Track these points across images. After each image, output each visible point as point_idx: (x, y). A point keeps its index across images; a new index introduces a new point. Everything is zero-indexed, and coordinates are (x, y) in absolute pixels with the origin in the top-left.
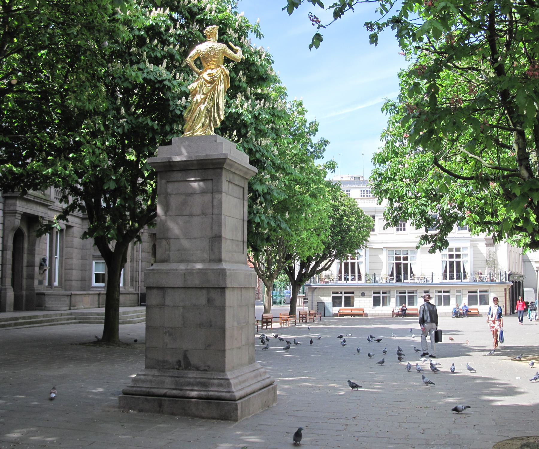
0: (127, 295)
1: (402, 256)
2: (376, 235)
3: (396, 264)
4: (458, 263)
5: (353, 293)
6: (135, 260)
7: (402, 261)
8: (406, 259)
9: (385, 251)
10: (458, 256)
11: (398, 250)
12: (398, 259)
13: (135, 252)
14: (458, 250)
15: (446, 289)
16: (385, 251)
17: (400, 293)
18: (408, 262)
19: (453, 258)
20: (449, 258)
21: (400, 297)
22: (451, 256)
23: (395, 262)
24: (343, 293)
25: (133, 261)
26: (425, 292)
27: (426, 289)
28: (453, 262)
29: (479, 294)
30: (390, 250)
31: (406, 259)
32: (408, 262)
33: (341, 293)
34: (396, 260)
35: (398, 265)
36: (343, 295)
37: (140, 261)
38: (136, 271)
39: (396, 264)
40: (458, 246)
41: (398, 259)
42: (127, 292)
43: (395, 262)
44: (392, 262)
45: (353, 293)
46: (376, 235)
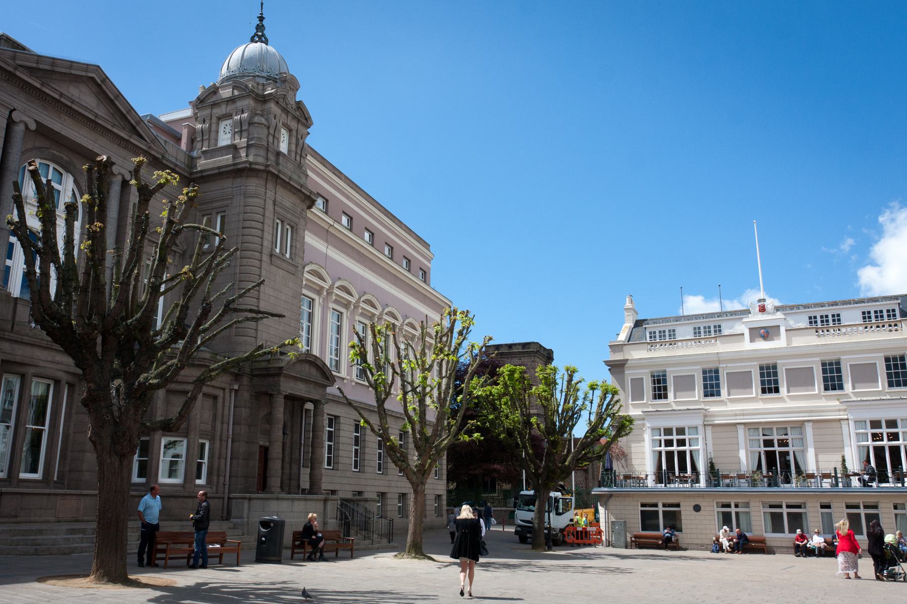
0: (186, 500)
1: (775, 437)
6: (218, 438)
7: (777, 448)
9: (741, 430)
10: (895, 436)
11: (767, 428)
12: (769, 443)
13: (218, 424)
16: (741, 430)
17: (771, 506)
18: (790, 449)
21: (772, 514)
22: (876, 437)
23: (763, 449)
24: (660, 505)
25: (214, 440)
26: (822, 507)
28: (883, 448)
30: (751, 427)
32: (790, 449)
35: (770, 456)
37: (230, 440)
38: (219, 458)
40: (891, 416)
41: (769, 443)
42: (186, 494)
43: (763, 449)
44: (759, 449)
45: (678, 505)
46: (722, 401)
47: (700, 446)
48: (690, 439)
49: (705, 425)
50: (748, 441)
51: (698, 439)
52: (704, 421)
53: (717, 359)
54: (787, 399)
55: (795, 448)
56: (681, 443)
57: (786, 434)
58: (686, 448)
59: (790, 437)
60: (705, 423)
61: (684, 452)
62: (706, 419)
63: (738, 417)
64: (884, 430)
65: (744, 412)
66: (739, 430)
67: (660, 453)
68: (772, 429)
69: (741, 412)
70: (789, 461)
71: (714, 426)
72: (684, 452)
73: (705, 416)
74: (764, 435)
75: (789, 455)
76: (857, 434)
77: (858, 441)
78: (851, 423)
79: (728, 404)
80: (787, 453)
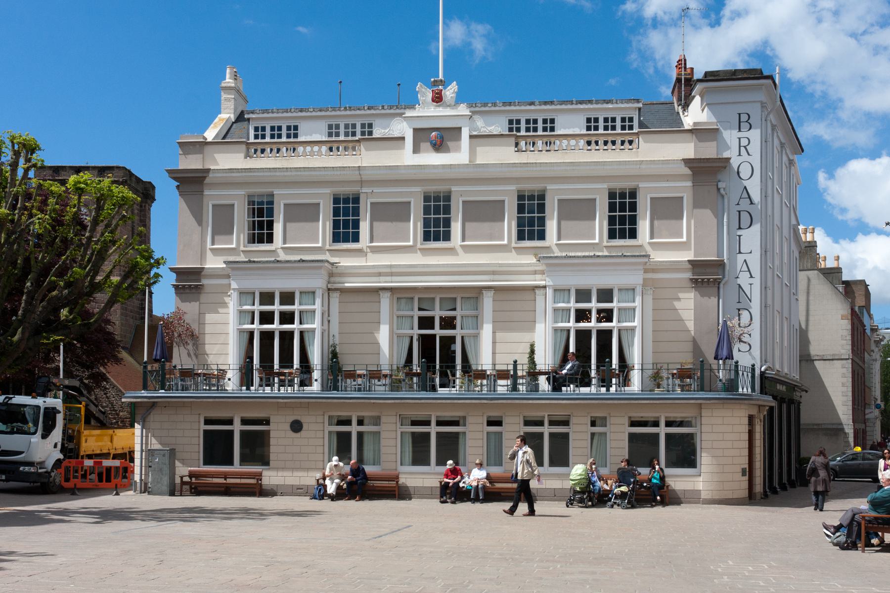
1: (438, 313)
2: (360, 251)
3: (423, 338)
4: (605, 337)
5: (267, 422)
7: (438, 331)
8: (448, 323)
9: (385, 301)
10: (606, 314)
12: (426, 322)
14: (606, 295)
15: (559, 413)
16: (385, 301)
18: (457, 333)
19: (588, 319)
20: (578, 320)
22: (582, 315)
23: (416, 332)
27: (495, 414)
29: (662, 431)
31: (448, 323)
32: (457, 333)
33: (230, 422)
34: (421, 327)
35: (427, 342)
36: (237, 428)
39: (423, 338)
43: (416, 332)
44: (410, 332)
46: (360, 251)
47: (315, 325)
48: (301, 312)
49: (329, 290)
50: (395, 318)
51: (314, 312)
52: (329, 283)
53: (358, 178)
54: (460, 250)
55: (464, 332)
56: (287, 318)
57: (455, 309)
58: (295, 327)
59: (458, 313)
60: (330, 286)
61: (291, 334)
62: (332, 279)
63: (382, 278)
64: (594, 305)
65: (394, 270)
66: (382, 300)
67: (251, 334)
68: (433, 299)
69: (388, 270)
70: (454, 352)
71: (344, 291)
72: (291, 334)
73: (331, 275)
74: (420, 309)
75: (455, 343)
76: (556, 310)
77: (556, 322)
78: (550, 292)
79: (370, 255)
80: (452, 339)
